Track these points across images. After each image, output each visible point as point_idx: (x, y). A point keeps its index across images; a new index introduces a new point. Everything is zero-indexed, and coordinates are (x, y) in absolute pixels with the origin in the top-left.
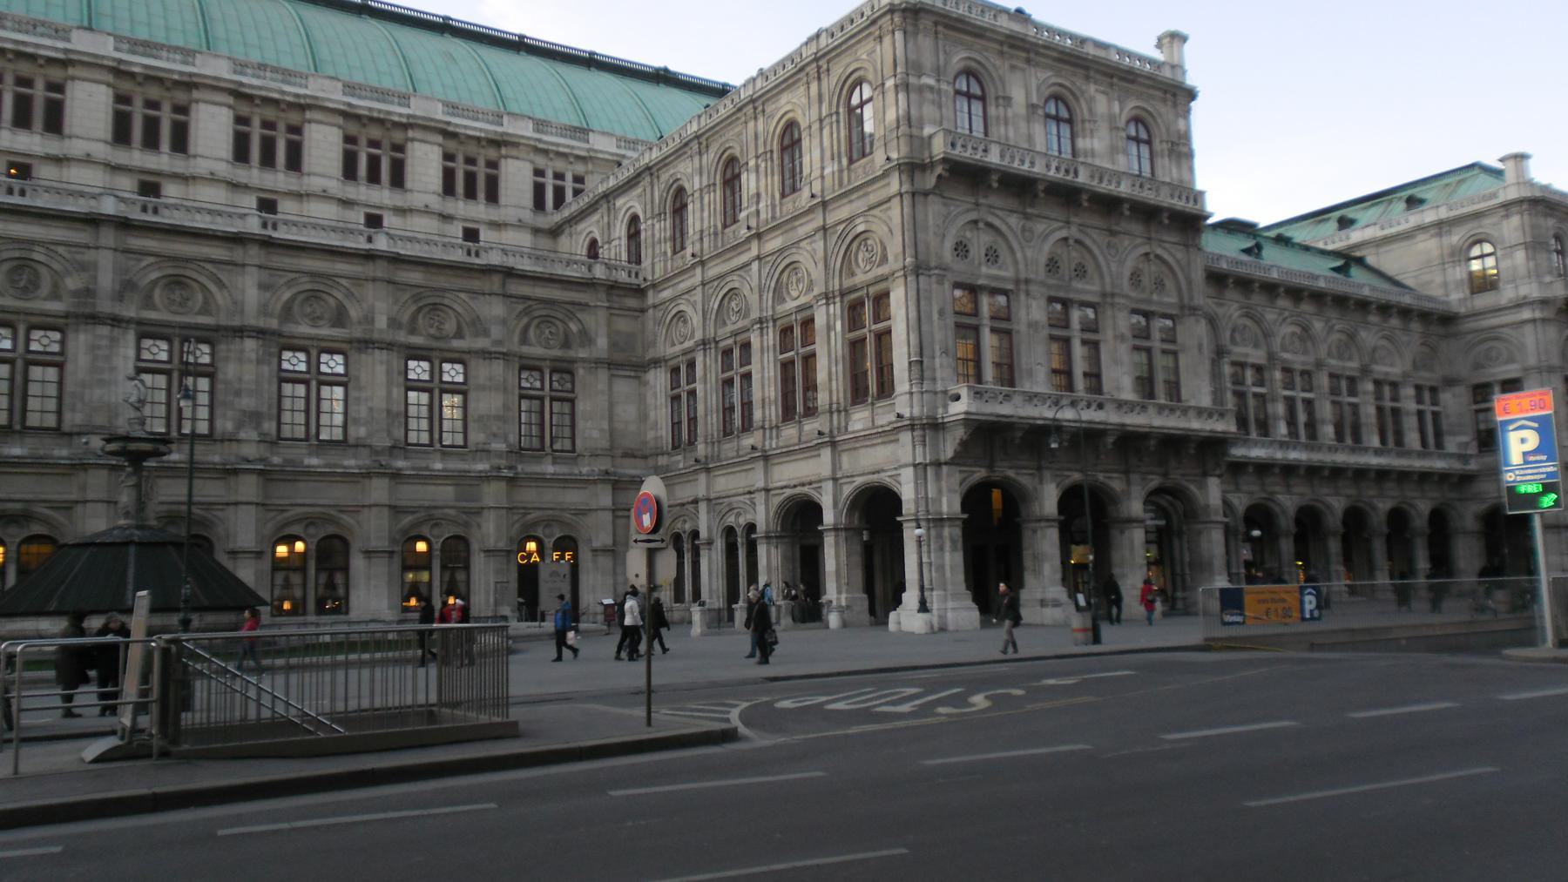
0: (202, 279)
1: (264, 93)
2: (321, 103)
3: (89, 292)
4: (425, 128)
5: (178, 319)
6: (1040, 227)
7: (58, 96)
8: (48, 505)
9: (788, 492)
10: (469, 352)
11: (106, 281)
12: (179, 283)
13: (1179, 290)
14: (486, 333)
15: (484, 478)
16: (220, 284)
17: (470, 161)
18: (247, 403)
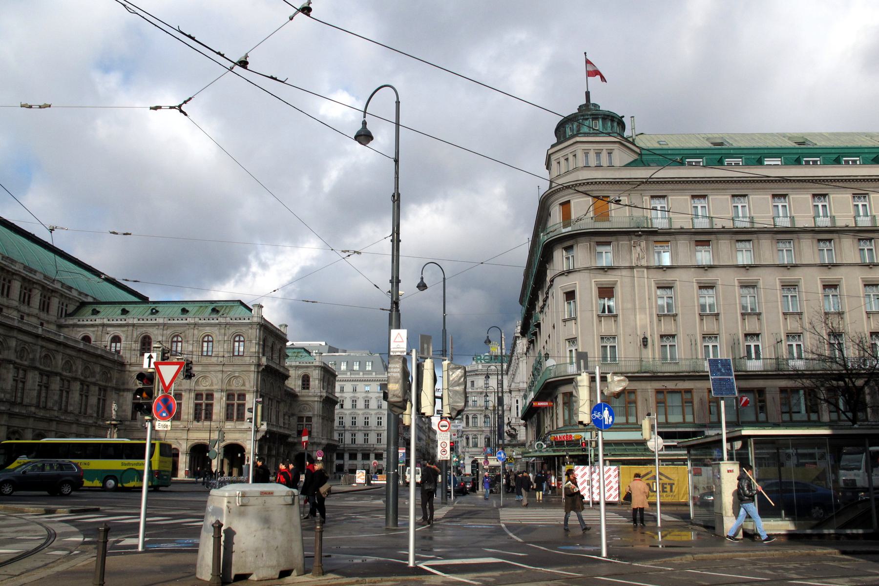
3: (33, 360)
4: (39, 284)
9: (196, 441)
14: (94, 376)
15: (91, 426)
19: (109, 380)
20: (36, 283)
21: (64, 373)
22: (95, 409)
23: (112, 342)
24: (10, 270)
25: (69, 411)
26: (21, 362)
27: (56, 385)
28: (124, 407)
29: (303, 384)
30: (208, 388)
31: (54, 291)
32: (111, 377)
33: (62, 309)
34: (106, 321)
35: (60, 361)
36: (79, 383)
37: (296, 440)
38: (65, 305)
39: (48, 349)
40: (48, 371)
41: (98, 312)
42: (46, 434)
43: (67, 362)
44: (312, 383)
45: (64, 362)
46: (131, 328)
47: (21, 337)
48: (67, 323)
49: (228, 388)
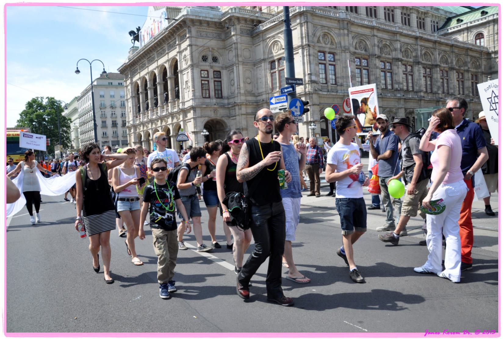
0: (430, 53)
10: (464, 71)
14: (467, 66)
21: (442, 65)
22: (471, 90)
23: (476, 39)
25: (450, 93)
27: (437, 75)
31: (426, 13)
32: (479, 65)
33: (434, 26)
34: (469, 25)
35: (438, 56)
36: (455, 71)
38: (436, 22)
39: (427, 48)
41: (462, 21)
45: (440, 56)
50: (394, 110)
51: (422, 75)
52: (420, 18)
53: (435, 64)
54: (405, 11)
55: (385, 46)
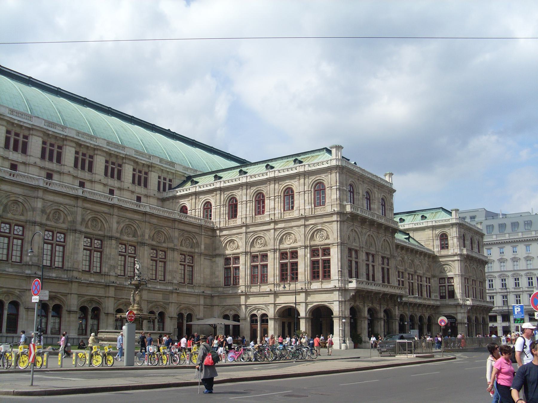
0: (102, 219)
1: (85, 144)
2: (102, 149)
3: (74, 222)
4: (130, 159)
5: (94, 232)
6: (364, 231)
7: (26, 140)
8: (61, 294)
11: (79, 219)
12: (95, 220)
13: (390, 250)
14: (172, 242)
15: (172, 292)
16: (107, 221)
17: (140, 172)
18: (112, 262)
19: (198, 245)
20: (125, 158)
21: (126, 238)
24: (89, 145)
26: (55, 224)
28: (217, 273)
29: (441, 245)
30: (292, 245)
31: (150, 166)
32: (197, 243)
33: (165, 184)
35: (115, 225)
37: (438, 303)
38: (168, 180)
40: (99, 235)
42: (101, 300)
43: (128, 226)
44: (450, 242)
45: (122, 225)
46: (218, 192)
47: (51, 197)
48: (168, 196)
49: (312, 243)
50: (17, 292)
51: (82, 247)
52: (140, 172)
53: (109, 235)
54: (114, 160)
55: (16, 202)
